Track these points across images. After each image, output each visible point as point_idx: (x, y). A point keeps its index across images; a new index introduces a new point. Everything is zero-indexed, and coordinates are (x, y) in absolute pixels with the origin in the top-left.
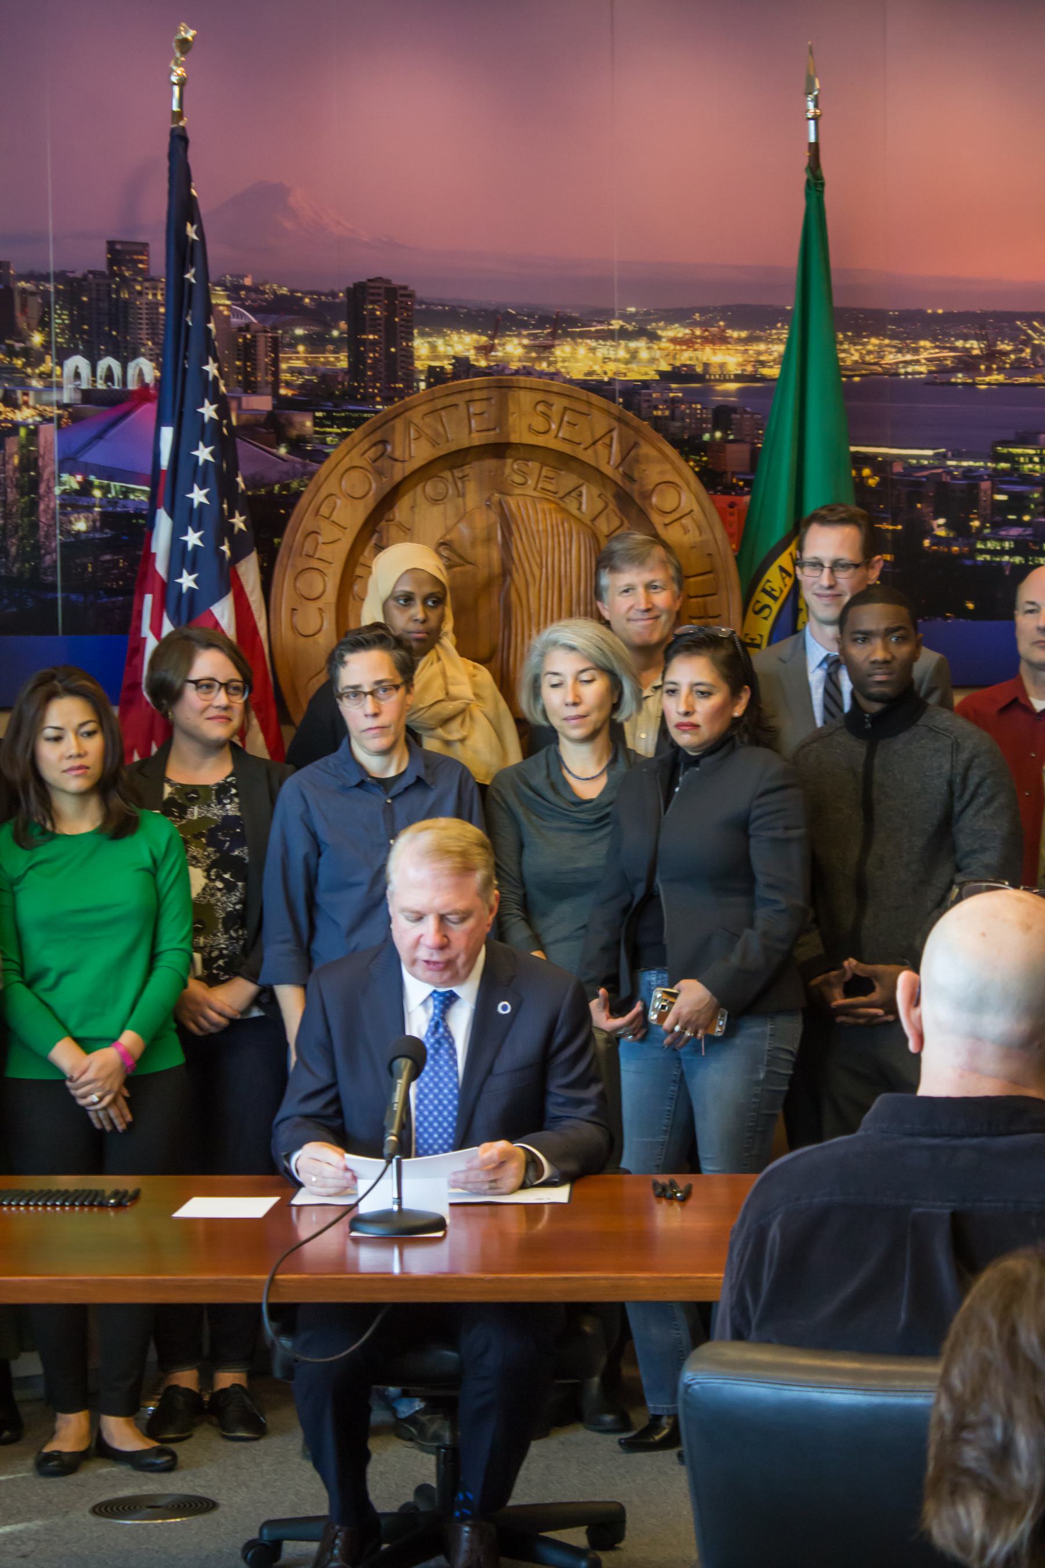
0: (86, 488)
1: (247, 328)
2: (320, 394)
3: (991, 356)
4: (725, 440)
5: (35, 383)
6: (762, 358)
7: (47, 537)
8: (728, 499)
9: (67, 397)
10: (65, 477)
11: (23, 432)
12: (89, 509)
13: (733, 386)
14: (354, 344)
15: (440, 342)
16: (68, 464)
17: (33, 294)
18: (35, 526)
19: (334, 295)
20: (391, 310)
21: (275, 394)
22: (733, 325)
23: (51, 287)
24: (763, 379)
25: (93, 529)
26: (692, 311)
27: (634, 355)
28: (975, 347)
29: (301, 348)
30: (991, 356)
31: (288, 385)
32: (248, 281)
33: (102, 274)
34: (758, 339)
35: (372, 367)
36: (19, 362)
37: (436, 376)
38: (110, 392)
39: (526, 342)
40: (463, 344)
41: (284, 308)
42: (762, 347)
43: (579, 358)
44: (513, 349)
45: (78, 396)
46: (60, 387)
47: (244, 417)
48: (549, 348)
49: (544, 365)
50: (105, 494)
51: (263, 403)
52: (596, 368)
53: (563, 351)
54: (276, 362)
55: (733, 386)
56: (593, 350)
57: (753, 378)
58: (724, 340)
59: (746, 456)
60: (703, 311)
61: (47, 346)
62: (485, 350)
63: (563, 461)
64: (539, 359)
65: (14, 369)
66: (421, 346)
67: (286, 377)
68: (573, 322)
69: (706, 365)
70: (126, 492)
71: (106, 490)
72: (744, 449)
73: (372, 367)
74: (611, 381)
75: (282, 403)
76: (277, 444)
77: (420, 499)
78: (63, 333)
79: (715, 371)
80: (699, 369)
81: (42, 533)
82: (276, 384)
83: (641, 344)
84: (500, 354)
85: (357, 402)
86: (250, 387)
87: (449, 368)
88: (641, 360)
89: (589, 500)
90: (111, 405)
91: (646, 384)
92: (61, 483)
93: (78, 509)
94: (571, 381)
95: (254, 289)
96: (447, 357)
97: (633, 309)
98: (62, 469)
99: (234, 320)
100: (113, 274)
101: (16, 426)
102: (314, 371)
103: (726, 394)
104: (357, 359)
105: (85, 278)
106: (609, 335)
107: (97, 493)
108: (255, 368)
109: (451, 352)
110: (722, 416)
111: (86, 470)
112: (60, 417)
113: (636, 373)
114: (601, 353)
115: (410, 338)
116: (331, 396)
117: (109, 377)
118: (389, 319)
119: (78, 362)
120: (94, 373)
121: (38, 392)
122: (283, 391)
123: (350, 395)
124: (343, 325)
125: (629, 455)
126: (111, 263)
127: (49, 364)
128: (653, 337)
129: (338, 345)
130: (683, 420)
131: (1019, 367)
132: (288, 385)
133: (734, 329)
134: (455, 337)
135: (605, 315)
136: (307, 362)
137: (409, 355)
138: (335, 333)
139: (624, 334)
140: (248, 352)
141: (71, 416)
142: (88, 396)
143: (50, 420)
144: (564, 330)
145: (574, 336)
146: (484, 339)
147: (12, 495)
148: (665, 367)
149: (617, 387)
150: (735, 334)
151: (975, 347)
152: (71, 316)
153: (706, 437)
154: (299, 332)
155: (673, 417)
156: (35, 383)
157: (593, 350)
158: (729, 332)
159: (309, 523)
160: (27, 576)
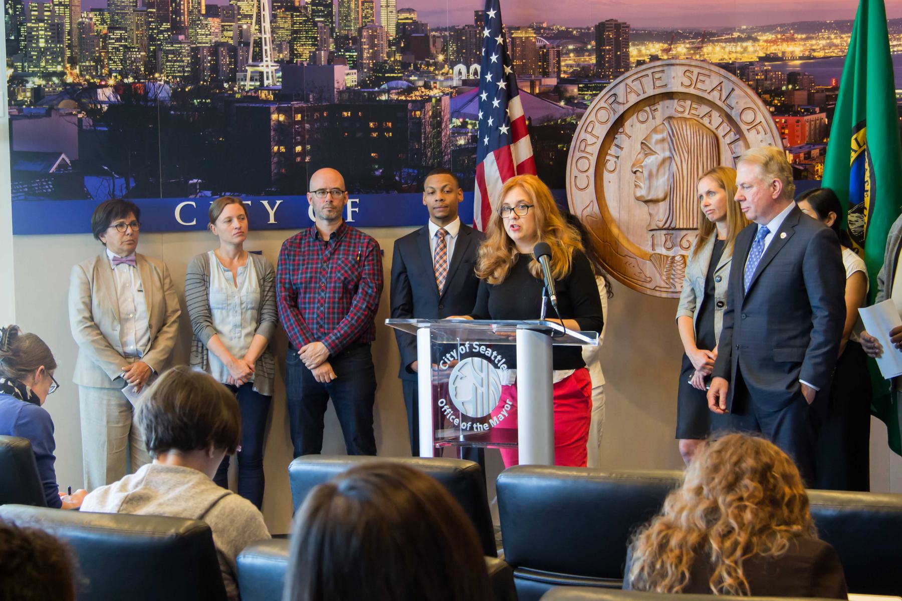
0: (464, 124)
1: (544, 47)
2: (582, 77)
4: (794, 89)
5: (440, 78)
6: (814, 48)
7: (445, 147)
8: (796, 118)
9: (456, 82)
10: (454, 120)
11: (434, 100)
12: (466, 134)
13: (798, 62)
14: (599, 51)
15: (643, 48)
16: (455, 113)
17: (438, 37)
18: (440, 143)
19: (589, 29)
20: (618, 34)
21: (558, 77)
22: (798, 31)
23: (447, 33)
24: (814, 58)
25: (468, 143)
26: (776, 26)
27: (745, 49)
29: (572, 55)
31: (565, 72)
32: (545, 25)
33: (472, 26)
34: (812, 38)
35: (608, 62)
36: (432, 69)
37: (640, 63)
38: (476, 80)
39: (688, 46)
40: (655, 48)
41: (564, 36)
42: (814, 42)
43: (716, 52)
44: (681, 49)
45: (461, 83)
46: (451, 79)
47: (542, 89)
49: (698, 57)
50: (473, 127)
51: (552, 82)
52: (726, 57)
53: (707, 49)
54: (559, 62)
55: (798, 62)
56: (724, 48)
57: (809, 58)
58: (793, 39)
59: (806, 97)
60: (782, 26)
61: (445, 61)
64: (695, 54)
65: (430, 72)
67: (563, 69)
68: (712, 35)
69: (784, 53)
71: (475, 125)
72: (805, 93)
73: (608, 62)
74: (732, 64)
75: (562, 81)
76: (560, 101)
78: (453, 54)
79: (788, 55)
80: (780, 55)
81: (443, 146)
82: (559, 72)
83: (749, 44)
84: (674, 52)
85: (600, 78)
86: (546, 74)
87: (648, 60)
88: (749, 52)
91: (751, 63)
92: (451, 123)
93: (460, 134)
94: (712, 63)
95: (548, 28)
96: (647, 55)
97: (744, 27)
98: (452, 117)
99: (538, 44)
100: (477, 26)
101: (430, 98)
102: (578, 65)
103: (795, 66)
104: (600, 59)
105: (464, 28)
106: (733, 40)
107: (470, 127)
108: (548, 66)
109: (648, 52)
110: (792, 77)
111: (465, 116)
112: (452, 93)
113: (746, 58)
114: (727, 50)
115: (627, 46)
116: (587, 77)
118: (617, 39)
119: (461, 67)
120: (468, 72)
121: (441, 82)
122: (562, 76)
123: (597, 76)
124: (593, 43)
126: (476, 21)
127: (446, 69)
128: (755, 40)
129: (590, 52)
130: (771, 80)
132: (565, 72)
133: (798, 33)
134: (651, 45)
135: (730, 30)
136: (574, 60)
137: (627, 55)
138: (589, 47)
139: (740, 39)
140: (545, 58)
141: (457, 92)
142: (465, 82)
143: (447, 94)
144: (708, 39)
145: (713, 42)
146: (666, 46)
147: (428, 129)
148: (762, 54)
149: (737, 65)
150: (799, 36)
152: (457, 45)
153: (784, 88)
154: (571, 47)
155: (766, 79)
156: (440, 78)
157: (724, 48)
158: (796, 36)
160: (436, 165)
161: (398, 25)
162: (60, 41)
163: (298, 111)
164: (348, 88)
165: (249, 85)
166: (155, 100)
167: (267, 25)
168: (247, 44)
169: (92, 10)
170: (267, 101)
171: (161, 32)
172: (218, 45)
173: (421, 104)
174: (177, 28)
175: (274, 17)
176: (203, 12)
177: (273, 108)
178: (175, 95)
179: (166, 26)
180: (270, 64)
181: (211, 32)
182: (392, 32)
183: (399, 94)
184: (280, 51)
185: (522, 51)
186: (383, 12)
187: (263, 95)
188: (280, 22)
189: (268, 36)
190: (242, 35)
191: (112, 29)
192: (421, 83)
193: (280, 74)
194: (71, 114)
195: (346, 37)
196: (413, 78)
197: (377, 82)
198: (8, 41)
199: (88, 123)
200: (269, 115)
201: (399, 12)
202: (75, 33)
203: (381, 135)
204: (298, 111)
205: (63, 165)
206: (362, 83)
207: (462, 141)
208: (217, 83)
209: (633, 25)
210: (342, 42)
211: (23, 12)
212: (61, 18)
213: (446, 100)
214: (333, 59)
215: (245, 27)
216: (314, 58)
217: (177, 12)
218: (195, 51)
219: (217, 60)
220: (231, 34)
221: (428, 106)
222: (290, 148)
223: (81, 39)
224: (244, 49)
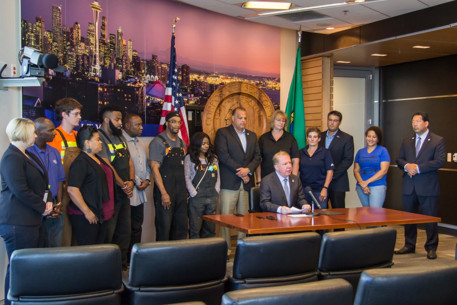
0: (149, 98)
3: (260, 83)
14: (182, 75)
16: (147, 94)
18: (143, 104)
20: (187, 70)
22: (229, 76)
27: (216, 80)
28: (258, 82)
30: (260, 83)
38: (152, 81)
44: (202, 78)
48: (206, 78)
60: (225, 73)
62: (199, 78)
63: (249, 96)
66: (191, 76)
70: (154, 99)
77: (227, 102)
83: (217, 78)
89: (253, 103)
90: (152, 84)
91: (218, 85)
101: (141, 86)
104: (183, 78)
106: (213, 77)
117: (152, 79)
119: (148, 76)
125: (260, 96)
127: (145, 76)
128: (219, 77)
131: (263, 86)
135: (213, 73)
139: (215, 77)
142: (150, 82)
151: (258, 82)
156: (143, 79)
159: (209, 105)
161: (133, 56)
162: (38, 44)
163: (106, 87)
164: (119, 80)
165: (93, 74)
166: (65, 76)
167: (98, 49)
168: (92, 56)
169: (48, 31)
170: (97, 82)
171: (67, 46)
172: (84, 55)
173: (138, 88)
174: (72, 45)
175: (100, 46)
176: (80, 40)
177: (99, 85)
178: (72, 75)
179: (69, 43)
180: (99, 66)
181: (82, 49)
182: (131, 59)
183: (133, 84)
184: (101, 61)
185: (164, 72)
186: (129, 51)
187: (96, 79)
188: (101, 48)
189: (98, 54)
190: (91, 52)
191: (54, 41)
192: (138, 81)
193: (101, 71)
195: (119, 58)
196: (136, 78)
197: (127, 78)
198: (22, 40)
199: (46, 84)
200: (98, 88)
201: (133, 51)
202: (43, 40)
203: (128, 100)
204: (106, 87)
205: (38, 104)
206: (123, 78)
207: (148, 105)
208: (83, 71)
209: (191, 67)
210: (118, 59)
211: (28, 27)
212: (39, 32)
214: (116, 67)
215: (92, 49)
216: (110, 65)
217: (72, 37)
218: (77, 56)
219: (83, 61)
220: (87, 51)
222: (103, 103)
223: (44, 44)
224: (90, 57)
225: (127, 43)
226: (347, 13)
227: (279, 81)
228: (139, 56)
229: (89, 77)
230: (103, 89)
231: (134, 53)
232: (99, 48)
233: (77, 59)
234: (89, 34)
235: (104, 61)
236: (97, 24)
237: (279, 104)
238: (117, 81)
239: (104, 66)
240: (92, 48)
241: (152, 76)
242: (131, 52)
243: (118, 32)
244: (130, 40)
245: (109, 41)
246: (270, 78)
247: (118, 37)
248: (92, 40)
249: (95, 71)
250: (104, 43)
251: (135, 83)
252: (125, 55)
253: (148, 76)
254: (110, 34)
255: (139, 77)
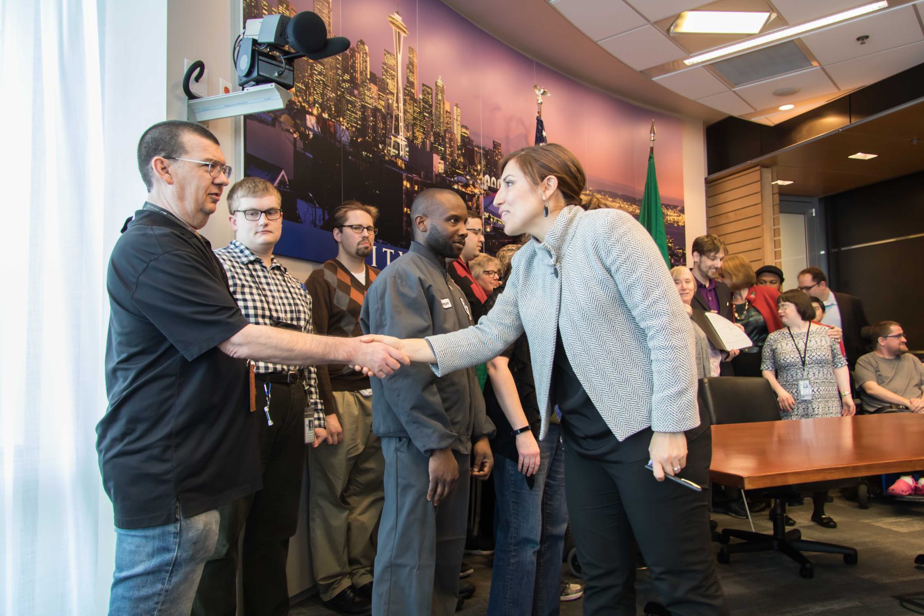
16: (486, 210)
119: (487, 177)
127: (481, 176)
142: (490, 188)
161: (462, 136)
164: (440, 174)
165: (393, 152)
166: (340, 141)
167: (401, 105)
168: (392, 117)
170: (401, 168)
171: (344, 81)
172: (376, 110)
175: (405, 100)
177: (404, 175)
178: (353, 143)
179: (347, 77)
182: (459, 140)
183: (462, 186)
187: (400, 162)
188: (408, 107)
189: (401, 115)
190: (389, 106)
192: (471, 182)
194: (289, 131)
197: (454, 174)
199: (300, 144)
201: (463, 126)
204: (417, 183)
206: (446, 172)
207: (488, 230)
210: (437, 135)
213: (482, 198)
214: (434, 150)
216: (424, 143)
217: (353, 67)
219: (376, 122)
221: (475, 200)
225: (452, 108)
226: (865, 41)
227: (682, 211)
228: (472, 138)
229: (385, 155)
230: (412, 186)
231: (464, 130)
232: (404, 105)
233: (363, 113)
234: (386, 71)
235: (413, 133)
236: (400, 57)
237: (684, 250)
238: (436, 175)
239: (412, 141)
240: (392, 100)
241: (493, 178)
242: (459, 127)
243: (436, 85)
244: (457, 106)
245: (421, 97)
246: (670, 206)
247: (437, 94)
248: (391, 85)
249: (397, 146)
250: (413, 99)
251: (466, 185)
252: (449, 130)
253: (487, 177)
254: (424, 85)
255: (472, 176)
